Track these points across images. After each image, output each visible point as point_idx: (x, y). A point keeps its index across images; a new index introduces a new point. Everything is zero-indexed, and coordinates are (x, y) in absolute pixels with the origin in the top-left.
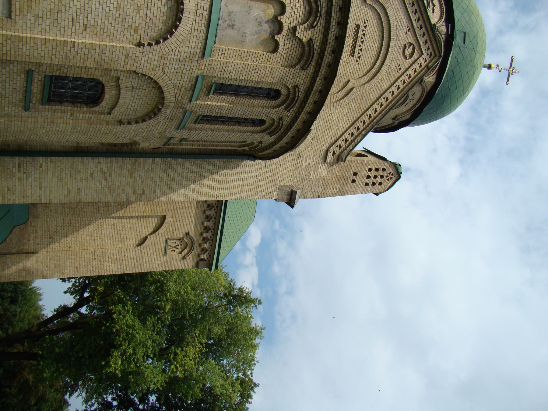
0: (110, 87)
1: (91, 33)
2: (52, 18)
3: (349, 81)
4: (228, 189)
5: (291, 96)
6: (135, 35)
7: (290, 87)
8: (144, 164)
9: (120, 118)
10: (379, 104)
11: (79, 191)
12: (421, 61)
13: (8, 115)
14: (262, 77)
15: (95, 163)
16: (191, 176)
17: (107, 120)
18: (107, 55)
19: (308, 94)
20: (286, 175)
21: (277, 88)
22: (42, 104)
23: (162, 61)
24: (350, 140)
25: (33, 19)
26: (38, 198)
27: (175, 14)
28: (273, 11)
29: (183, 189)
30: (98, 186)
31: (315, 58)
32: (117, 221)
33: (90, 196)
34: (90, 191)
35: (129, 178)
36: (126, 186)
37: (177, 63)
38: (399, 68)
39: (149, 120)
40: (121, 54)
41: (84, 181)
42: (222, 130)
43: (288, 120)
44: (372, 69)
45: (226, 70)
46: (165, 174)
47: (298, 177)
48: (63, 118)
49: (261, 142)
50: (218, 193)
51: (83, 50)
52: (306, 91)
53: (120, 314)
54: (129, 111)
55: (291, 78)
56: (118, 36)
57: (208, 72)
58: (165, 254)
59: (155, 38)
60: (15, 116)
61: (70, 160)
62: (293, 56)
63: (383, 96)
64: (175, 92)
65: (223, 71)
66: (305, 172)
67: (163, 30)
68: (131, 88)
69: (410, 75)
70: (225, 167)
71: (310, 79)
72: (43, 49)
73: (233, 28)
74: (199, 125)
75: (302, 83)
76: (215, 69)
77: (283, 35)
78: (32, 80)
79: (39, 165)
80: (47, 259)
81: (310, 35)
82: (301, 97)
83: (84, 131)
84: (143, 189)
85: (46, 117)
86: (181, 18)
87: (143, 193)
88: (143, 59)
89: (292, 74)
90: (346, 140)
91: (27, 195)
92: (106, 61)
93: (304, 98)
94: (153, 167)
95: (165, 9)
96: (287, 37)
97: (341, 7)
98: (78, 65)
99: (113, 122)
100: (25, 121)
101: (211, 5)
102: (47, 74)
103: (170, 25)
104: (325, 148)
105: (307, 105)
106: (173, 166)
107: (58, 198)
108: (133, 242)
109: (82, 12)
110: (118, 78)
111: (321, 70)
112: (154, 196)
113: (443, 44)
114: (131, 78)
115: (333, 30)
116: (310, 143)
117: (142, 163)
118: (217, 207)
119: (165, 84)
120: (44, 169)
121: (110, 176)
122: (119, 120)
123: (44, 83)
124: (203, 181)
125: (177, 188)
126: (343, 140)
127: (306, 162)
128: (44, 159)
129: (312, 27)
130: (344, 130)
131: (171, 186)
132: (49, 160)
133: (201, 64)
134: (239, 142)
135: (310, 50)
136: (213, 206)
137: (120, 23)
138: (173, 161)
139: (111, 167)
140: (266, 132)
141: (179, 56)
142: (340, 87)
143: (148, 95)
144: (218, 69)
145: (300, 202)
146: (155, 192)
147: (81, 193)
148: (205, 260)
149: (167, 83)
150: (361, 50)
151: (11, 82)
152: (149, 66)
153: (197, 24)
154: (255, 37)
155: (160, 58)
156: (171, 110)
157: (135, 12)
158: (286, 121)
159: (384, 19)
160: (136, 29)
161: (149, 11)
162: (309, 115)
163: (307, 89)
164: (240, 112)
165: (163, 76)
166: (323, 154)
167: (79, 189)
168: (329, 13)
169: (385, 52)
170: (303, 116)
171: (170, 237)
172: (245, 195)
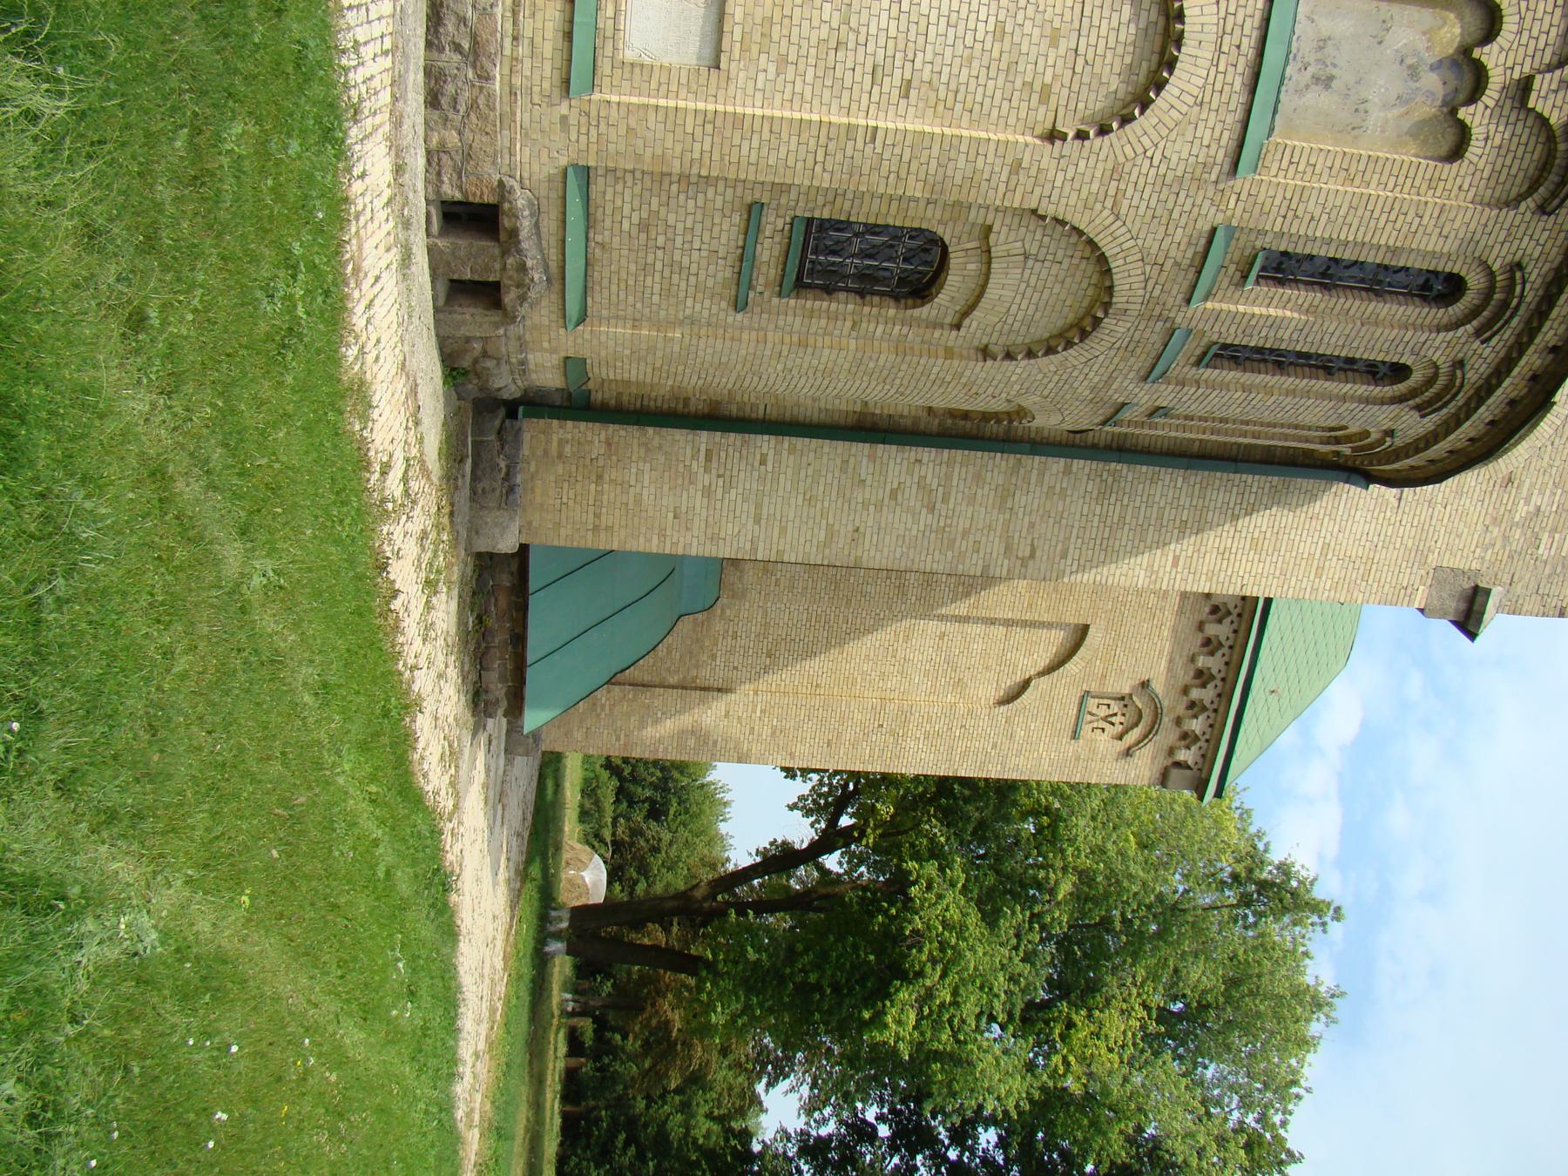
2: (821, 64)
4: (1279, 565)
5: (1497, 296)
6: (1042, 109)
8: (1042, 474)
9: (985, 340)
11: (856, 535)
13: (692, 321)
14: (1410, 236)
15: (905, 462)
16: (1172, 517)
17: (950, 344)
18: (961, 163)
20: (1460, 536)
21: (1455, 271)
22: (780, 295)
23: (1114, 184)
25: (772, 68)
26: (748, 546)
27: (1157, 48)
29: (1146, 555)
30: (909, 526)
32: (950, 627)
33: (886, 550)
34: (887, 538)
35: (995, 512)
36: (985, 532)
37: (1157, 188)
39: (1065, 349)
40: (999, 161)
41: (872, 508)
42: (1276, 392)
43: (1482, 370)
46: (1099, 507)
47: (1497, 546)
49: (1390, 433)
50: (1247, 576)
51: (897, 151)
52: (1549, 279)
53: (929, 888)
54: (1010, 321)
55: (1501, 239)
56: (995, 112)
57: (1246, 216)
58: (1075, 735)
59: (1098, 118)
60: (709, 325)
61: (839, 451)
62: (1513, 171)
64: (1144, 273)
65: (1291, 214)
67: (1121, 95)
68: (1022, 258)
70: (1276, 500)
72: (793, 147)
73: (1328, 87)
74: (1209, 371)
75: (1536, 254)
76: (1266, 209)
77: (1487, 107)
79: (758, 457)
80: (754, 711)
82: (1528, 299)
83: (885, 373)
84: (1032, 545)
85: (788, 329)
87: (1032, 556)
88: (1060, 176)
89: (1506, 226)
91: (722, 535)
92: (958, 180)
93: (1539, 304)
94: (1064, 485)
98: (881, 190)
99: (965, 353)
100: (733, 339)
101: (1266, 20)
103: (1142, 79)
105: (1548, 324)
106: (1123, 484)
107: (801, 548)
108: (989, 691)
109: (901, 46)
110: (988, 229)
112: (1062, 567)
114: (1023, 230)
116: (1549, 444)
117: (1035, 472)
118: (1239, 615)
119: (1118, 250)
120: (770, 468)
121: (945, 500)
122: (981, 346)
123: (790, 238)
124: (1206, 536)
125: (1129, 549)
127: (1527, 501)
131: (1111, 543)
132: (786, 445)
133: (1227, 193)
134: (1323, 429)
136: (1229, 613)
137: (1002, 76)
138: (1125, 471)
139: (949, 477)
140: (1411, 402)
141: (1162, 170)
143: (1068, 280)
144: (1275, 209)
145: (1496, 624)
146: (1064, 555)
147: (861, 541)
148: (1189, 768)
149: (1125, 246)
152: (1074, 195)
153: (1220, 77)
154: (1396, 112)
155: (1108, 173)
157: (1045, 42)
158: (1475, 373)
161: (1083, 41)
162: (1551, 356)
164: (1334, 340)
167: (857, 530)
171: (1094, 687)
172: (1327, 587)
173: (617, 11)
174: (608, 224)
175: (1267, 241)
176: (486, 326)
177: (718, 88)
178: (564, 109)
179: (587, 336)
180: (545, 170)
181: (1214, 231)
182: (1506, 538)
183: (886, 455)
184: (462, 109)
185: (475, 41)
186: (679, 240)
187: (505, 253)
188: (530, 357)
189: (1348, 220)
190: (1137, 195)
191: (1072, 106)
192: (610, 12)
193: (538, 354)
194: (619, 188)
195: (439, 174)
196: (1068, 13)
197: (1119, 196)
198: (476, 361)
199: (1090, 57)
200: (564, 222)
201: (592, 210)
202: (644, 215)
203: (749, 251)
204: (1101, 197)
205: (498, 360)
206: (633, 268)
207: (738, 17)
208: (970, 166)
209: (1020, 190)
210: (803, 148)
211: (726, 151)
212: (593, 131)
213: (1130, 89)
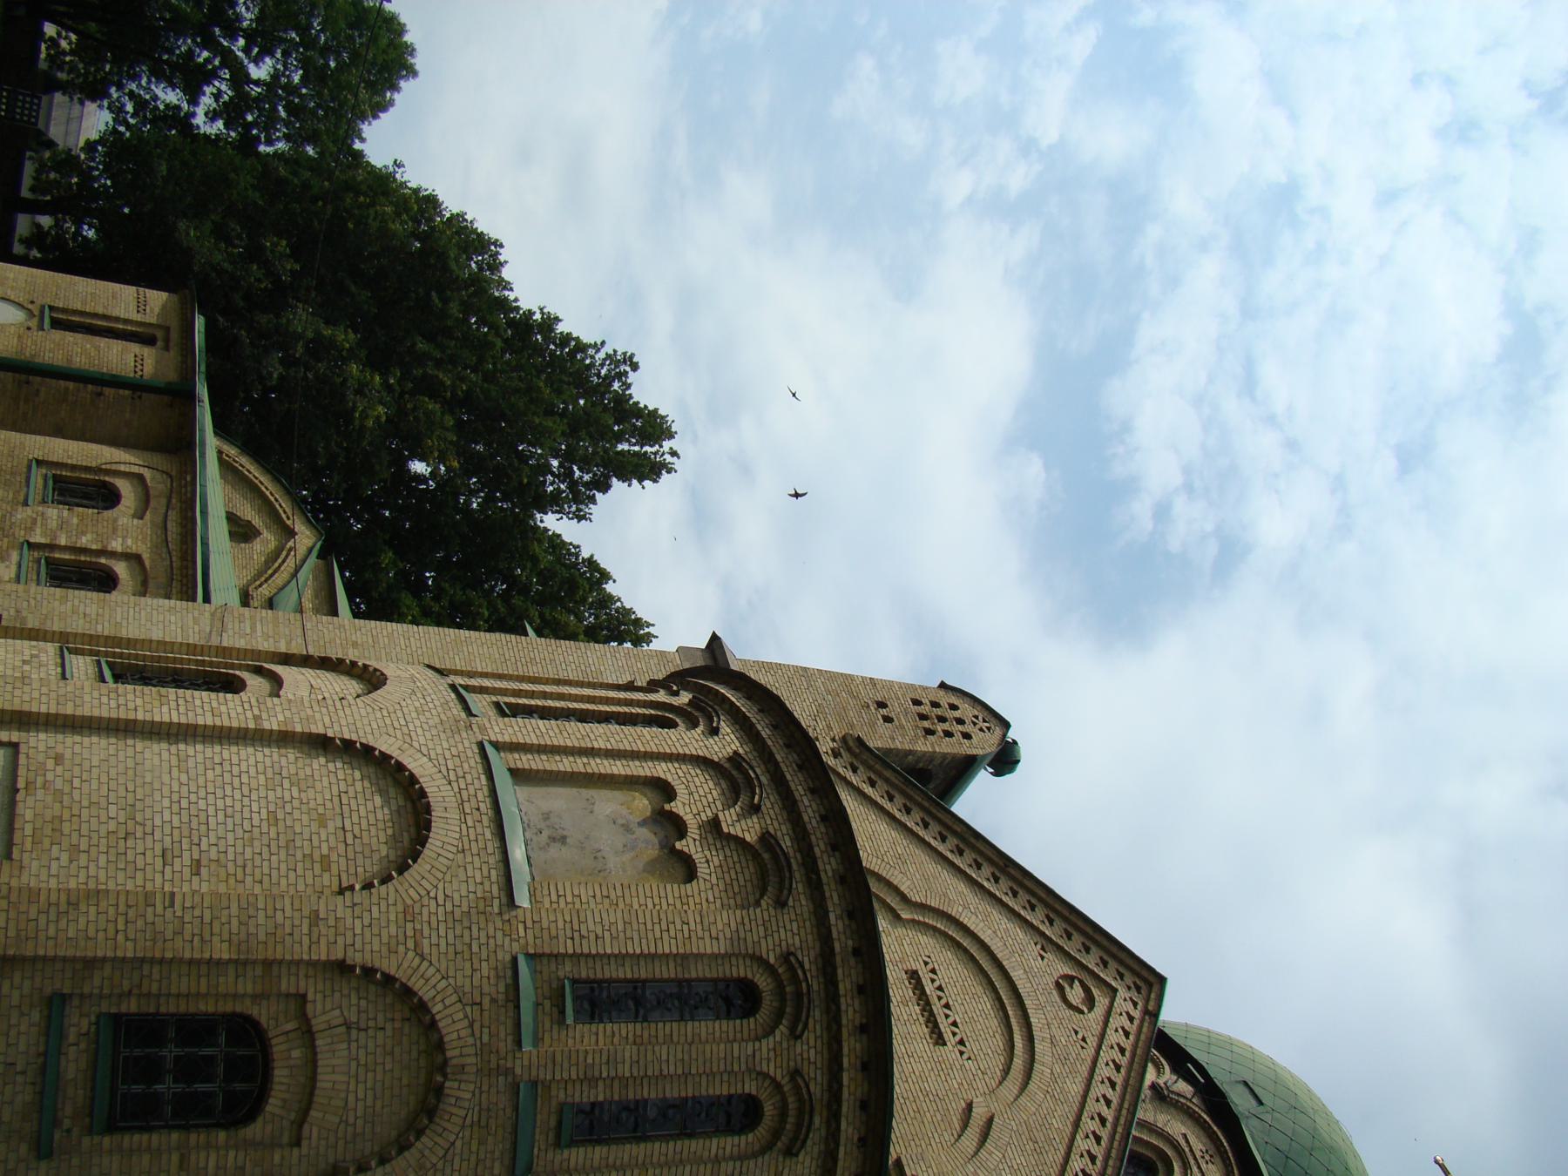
1: (213, 879)
2: (112, 851)
3: (970, 1106)
5: (788, 989)
6: (326, 876)
7: (772, 960)
9: (331, 1160)
10: (1087, 1137)
12: (1122, 1004)
14: (687, 942)
21: (742, 974)
23: (409, 925)
25: (65, 857)
28: (647, 802)
31: (797, 875)
37: (450, 925)
38: (1080, 1036)
39: (418, 1138)
40: (297, 915)
45: (584, 932)
51: (197, 913)
52: (820, 965)
54: (351, 1120)
55: (762, 934)
56: (283, 882)
62: (742, 883)
65: (576, 935)
67: (392, 858)
68: (343, 1029)
69: (1118, 1045)
71: (815, 930)
76: (554, 933)
77: (695, 840)
78: (62, 1035)
81: (757, 826)
82: (815, 987)
86: (430, 822)
88: (358, 922)
89: (760, 922)
92: (262, 937)
95: (384, 814)
96: (704, 842)
97: (799, 762)
98: (187, 955)
102: (104, 1010)
105: (842, 1000)
109: (186, 833)
110: (302, 998)
111: (827, 894)
113: (1208, 1119)
114: (337, 995)
115: (807, 803)
119: (433, 992)
123: (97, 1042)
129: (755, 809)
133: (514, 922)
135: (775, 857)
140: (779, 1144)
141: (449, 908)
142: (957, 1126)
143: (397, 1049)
144: (561, 933)
150: (961, 1042)
152: (376, 940)
153: (471, 831)
154: (627, 857)
155: (401, 916)
156: (472, 1087)
160: (326, 862)
162: (865, 1038)
163: (820, 960)
169: (1020, 1013)
170: (852, 1048)
175: (567, 969)
177: (11, 876)
181: (515, 960)
189: (629, 934)
190: (434, 934)
191: (352, 871)
196: (329, 805)
197: (418, 934)
199: (357, 831)
207: (29, 815)
208: (271, 923)
209: (323, 941)
210: (102, 917)
211: (22, 926)
213: (399, 853)
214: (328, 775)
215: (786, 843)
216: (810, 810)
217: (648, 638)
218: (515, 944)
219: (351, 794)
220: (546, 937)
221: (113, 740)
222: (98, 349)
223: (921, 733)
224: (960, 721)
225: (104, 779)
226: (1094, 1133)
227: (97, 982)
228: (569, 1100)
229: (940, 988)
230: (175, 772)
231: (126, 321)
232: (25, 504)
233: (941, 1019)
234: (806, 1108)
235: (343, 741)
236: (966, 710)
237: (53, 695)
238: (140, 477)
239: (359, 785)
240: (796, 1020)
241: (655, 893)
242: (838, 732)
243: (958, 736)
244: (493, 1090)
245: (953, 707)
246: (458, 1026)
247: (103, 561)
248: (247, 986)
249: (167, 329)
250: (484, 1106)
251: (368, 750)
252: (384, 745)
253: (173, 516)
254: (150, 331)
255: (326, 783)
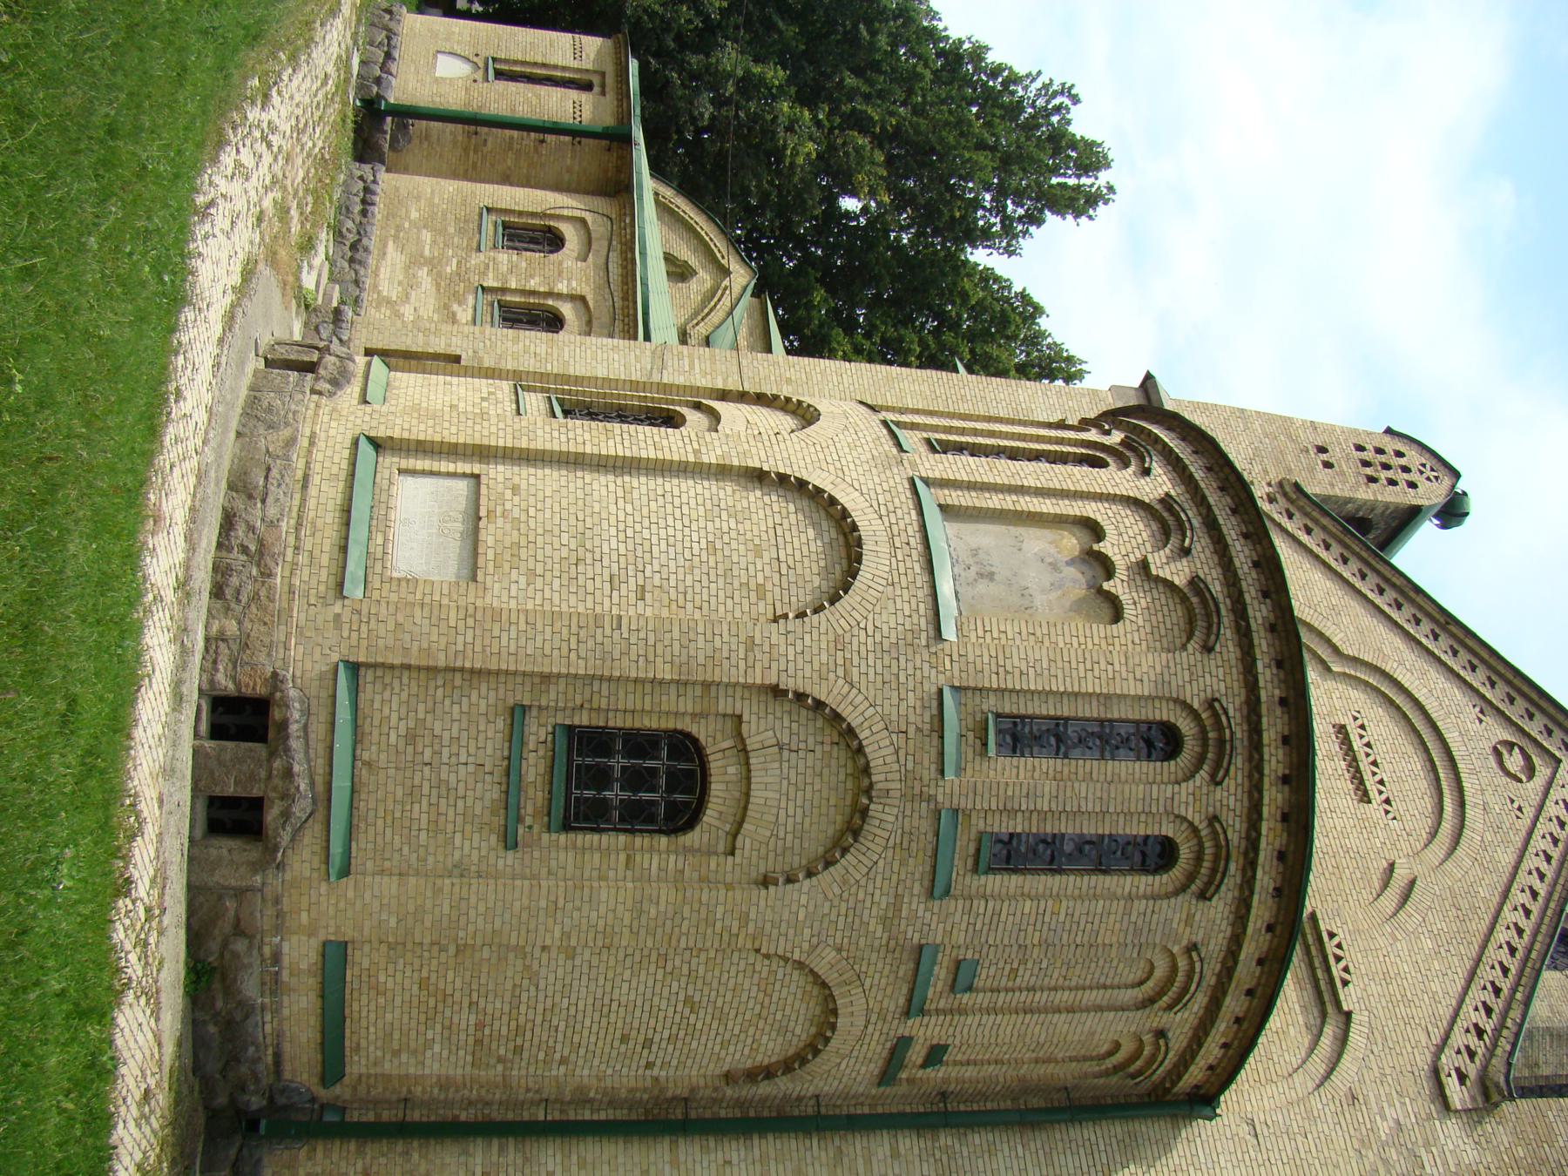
0: (720, 755)
1: (657, 604)
2: (565, 575)
3: (1392, 866)
5: (1211, 735)
6: (761, 604)
7: (1196, 706)
8: (868, 1162)
9: (762, 870)
13: (460, 870)
15: (713, 1165)
18: (701, 644)
19: (1254, 718)
21: (1165, 718)
22: (549, 830)
24: (1488, 1026)
25: (523, 580)
27: (844, 554)
38: (1516, 805)
39: (843, 856)
40: (734, 640)
44: (1439, 824)
45: (1009, 668)
48: (607, 879)
49: (1192, 948)
52: (1245, 712)
54: (781, 835)
56: (721, 608)
57: (964, 675)
61: (636, 1160)
63: (1515, 885)
65: (1001, 670)
66: (1399, 1153)
68: (776, 749)
72: (548, 636)
75: (1223, 690)
76: (979, 668)
78: (523, 743)
82: (1239, 735)
90: (1480, 1033)
92: (701, 660)
93: (1250, 738)
95: (816, 546)
98: (633, 674)
104: (1423, 1060)
105: (1266, 750)
106: (960, 1162)
109: (631, 560)
111: (1256, 642)
119: (861, 719)
126: (1468, 1031)
127: (1384, 1118)
128: (559, 1157)
129: (1186, 552)
130: (1454, 1003)
132: (574, 1158)
133: (940, 654)
135: (1204, 602)
137: (721, 580)
138: (957, 1146)
140: (1193, 887)
141: (878, 639)
143: (826, 771)
149: (867, 714)
150: (1387, 801)
151: (472, 743)
152: (808, 667)
154: (1053, 595)
155: (832, 645)
159: (1399, 700)
160: (761, 591)
162: (1286, 788)
165: (852, 695)
166: (1427, 1086)
168: (1211, 525)
170: (1273, 798)
173: (386, 540)
174: (376, 733)
175: (991, 704)
176: (242, 869)
178: (337, 608)
179: (350, 894)
180: (317, 667)
181: (940, 692)
182: (1385, 1162)
183: (690, 1159)
184: (244, 599)
185: (261, 543)
186: (446, 751)
187: (272, 754)
188: (286, 947)
190: (863, 663)
192: (380, 540)
193: (295, 938)
194: (387, 694)
195: (215, 662)
196: (764, 537)
198: (225, 944)
200: (333, 724)
201: (360, 722)
202: (412, 724)
203: (514, 763)
204: (832, 667)
205: (251, 937)
206: (399, 792)
209: (758, 665)
211: (487, 642)
212: (364, 628)
214: (764, 507)
215: (1217, 588)
216: (1242, 554)
217: (1080, 375)
218: (941, 677)
219: (786, 526)
220: (971, 670)
221: (564, 472)
222: (539, 97)
223: (1363, 480)
224: (1406, 469)
225: (557, 509)
226: (1523, 906)
227: (553, 696)
228: (989, 829)
229: (1368, 745)
230: (621, 502)
231: (564, 68)
232: (479, 250)
233: (1367, 776)
234: (1222, 854)
235: (779, 475)
236: (1413, 458)
237: (509, 430)
238: (583, 221)
239: (793, 517)
240: (1217, 765)
241: (1081, 632)
242: (1274, 477)
243: (1402, 485)
244: (916, 815)
245: (1399, 454)
246: (883, 752)
247: (550, 302)
248: (687, 705)
249: (603, 74)
250: (907, 829)
251: (802, 484)
252: (816, 479)
253: (614, 256)
254: (586, 77)
255: (762, 516)
